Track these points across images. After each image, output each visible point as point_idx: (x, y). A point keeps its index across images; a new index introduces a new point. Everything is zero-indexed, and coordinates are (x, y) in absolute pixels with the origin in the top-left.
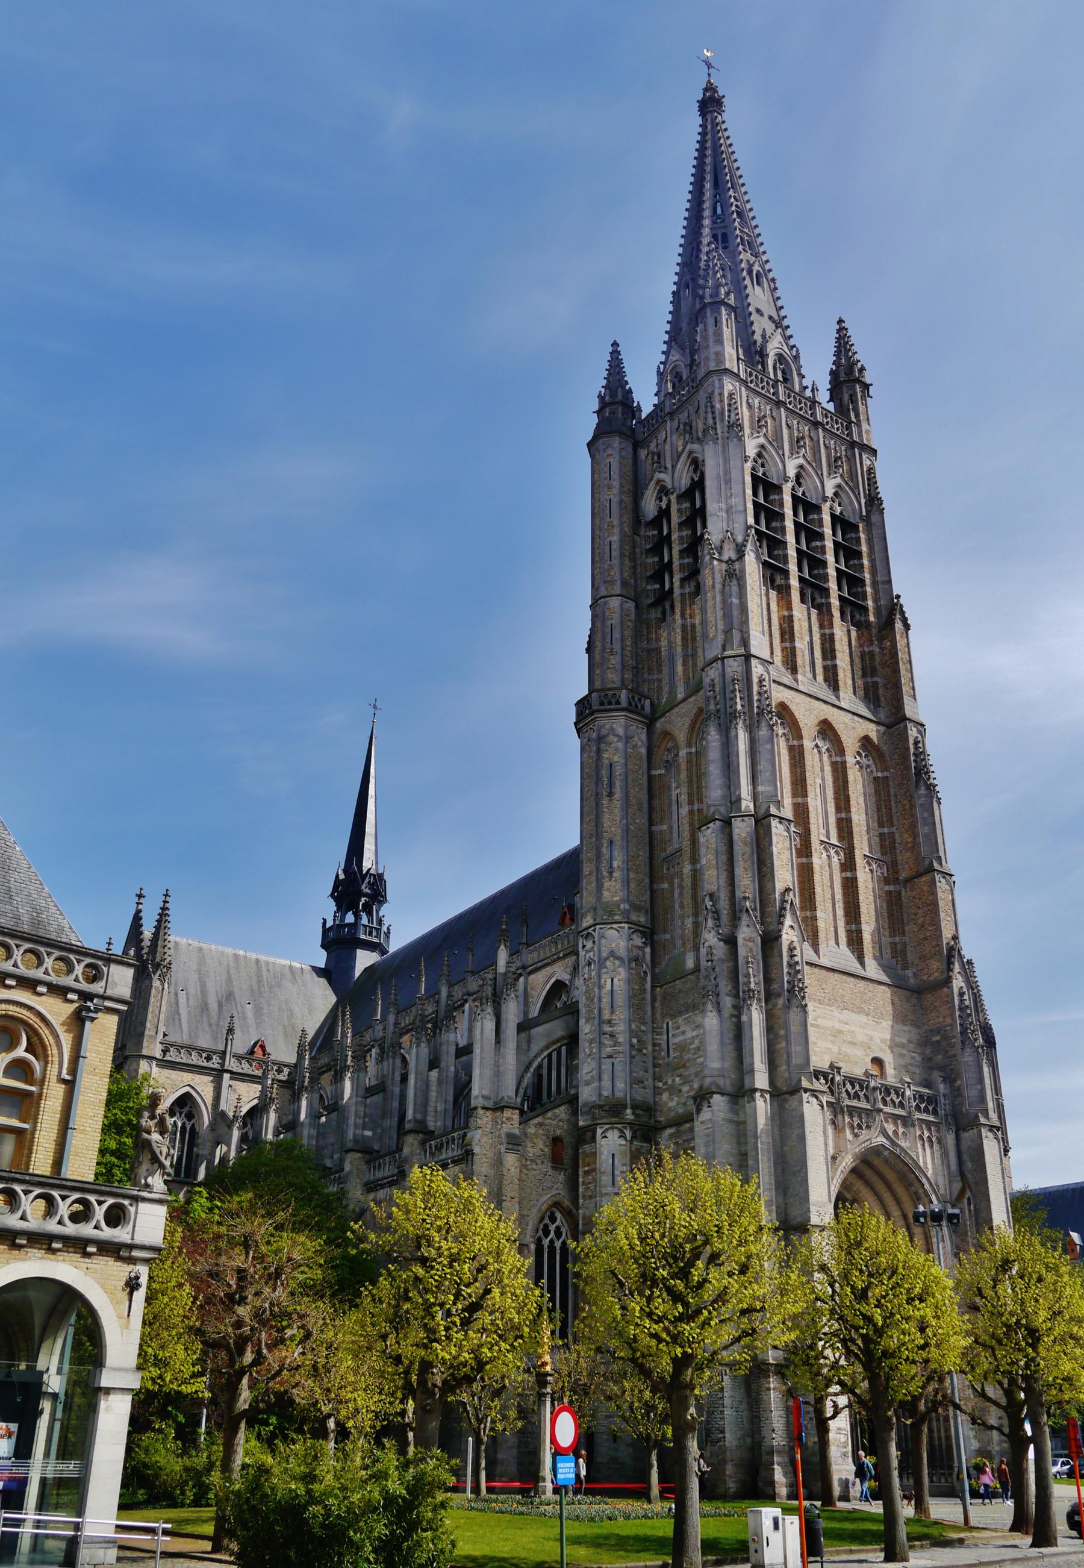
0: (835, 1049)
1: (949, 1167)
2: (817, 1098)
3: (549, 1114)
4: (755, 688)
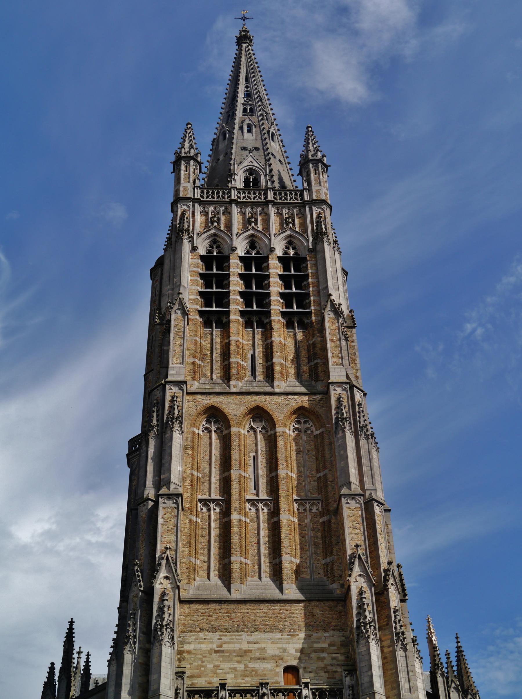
0: (241, 667)
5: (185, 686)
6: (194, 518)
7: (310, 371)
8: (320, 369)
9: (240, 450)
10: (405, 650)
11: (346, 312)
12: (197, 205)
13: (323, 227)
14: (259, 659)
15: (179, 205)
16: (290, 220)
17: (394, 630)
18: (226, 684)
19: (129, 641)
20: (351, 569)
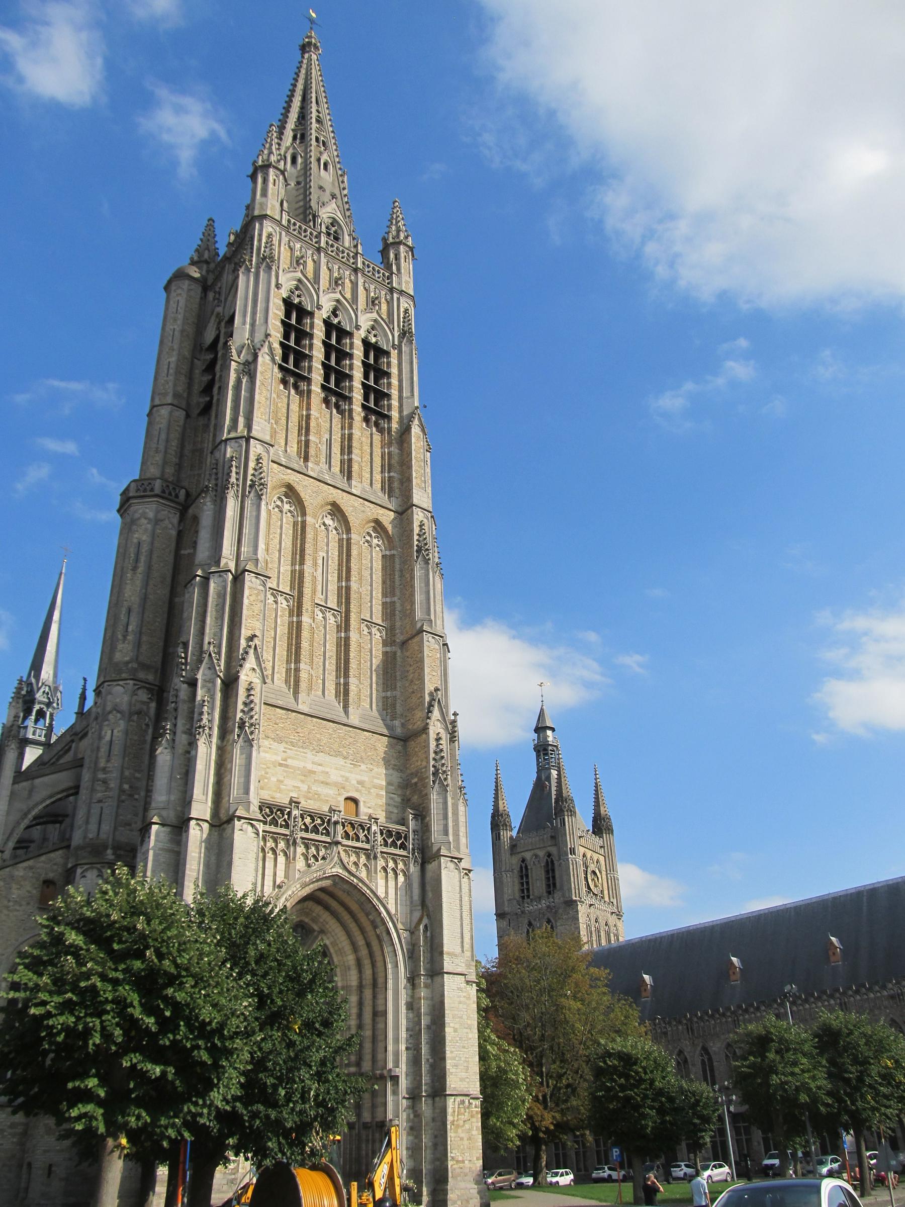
0: (304, 787)
1: (411, 897)
3: (43, 858)
4: (252, 464)
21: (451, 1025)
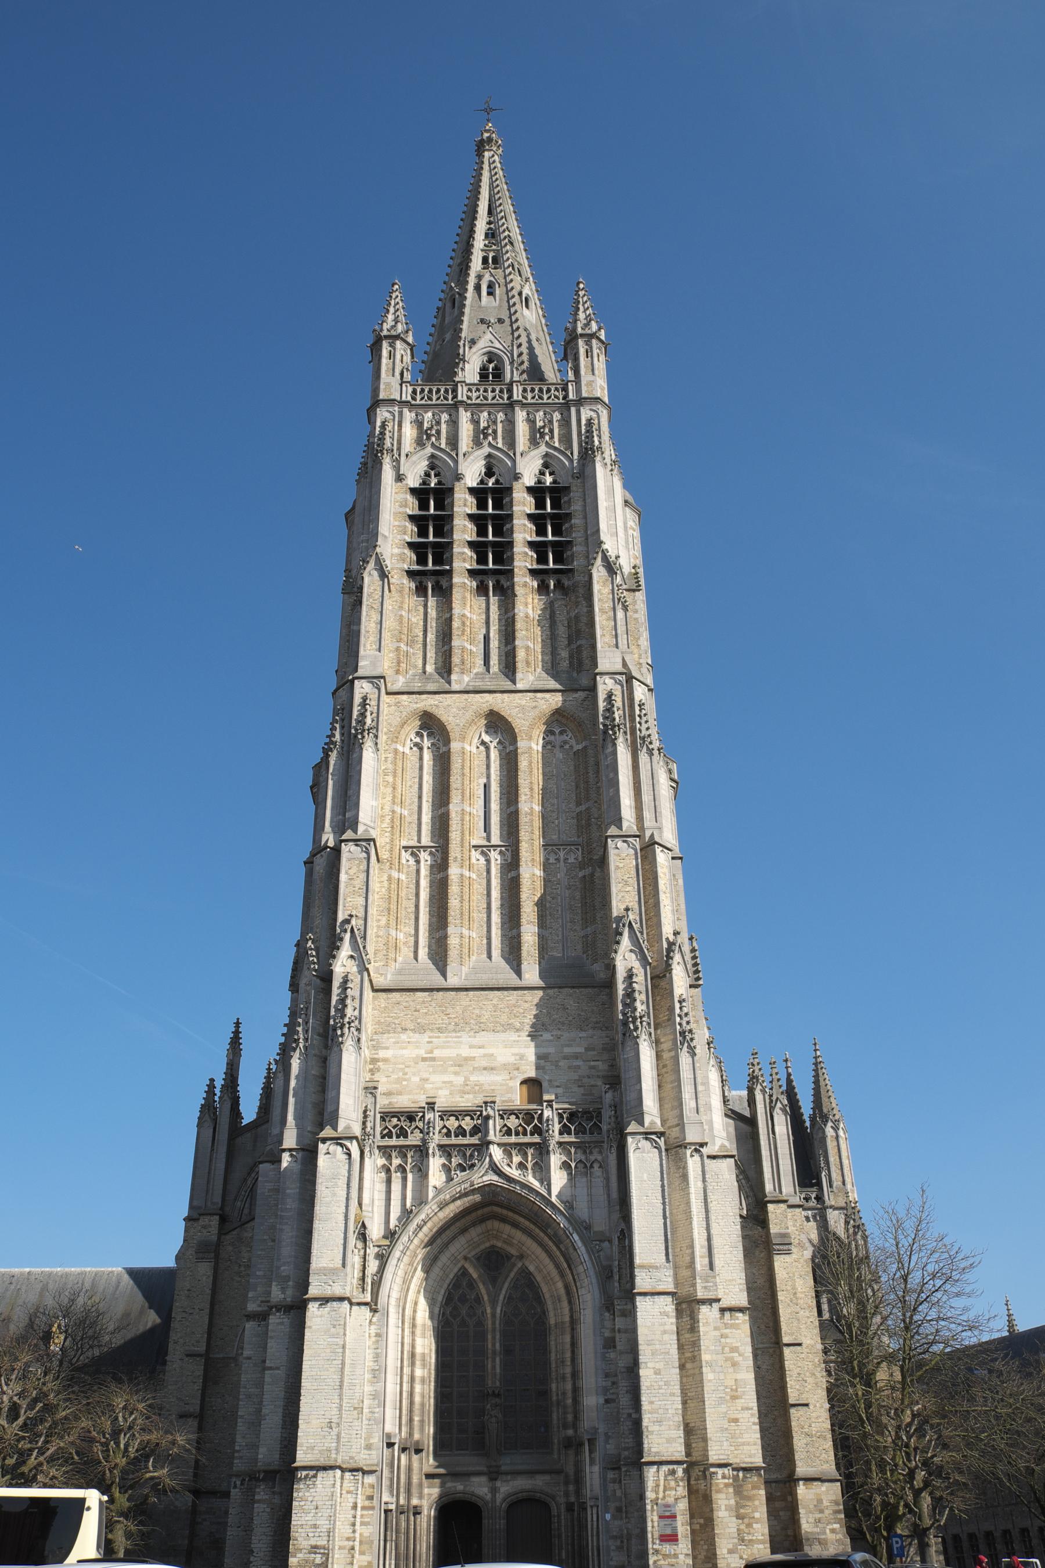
0: (459, 1080)
1: (609, 1195)
2: (341, 1145)
5: (378, 1106)
6: (395, 874)
7: (571, 657)
8: (585, 654)
9: (463, 774)
10: (692, 1052)
11: (627, 569)
12: (406, 411)
13: (596, 439)
14: (485, 1069)
15: (378, 412)
16: (547, 430)
17: (678, 1027)
18: (434, 1103)
19: (297, 1045)
20: (618, 943)
21: (649, 1365)
